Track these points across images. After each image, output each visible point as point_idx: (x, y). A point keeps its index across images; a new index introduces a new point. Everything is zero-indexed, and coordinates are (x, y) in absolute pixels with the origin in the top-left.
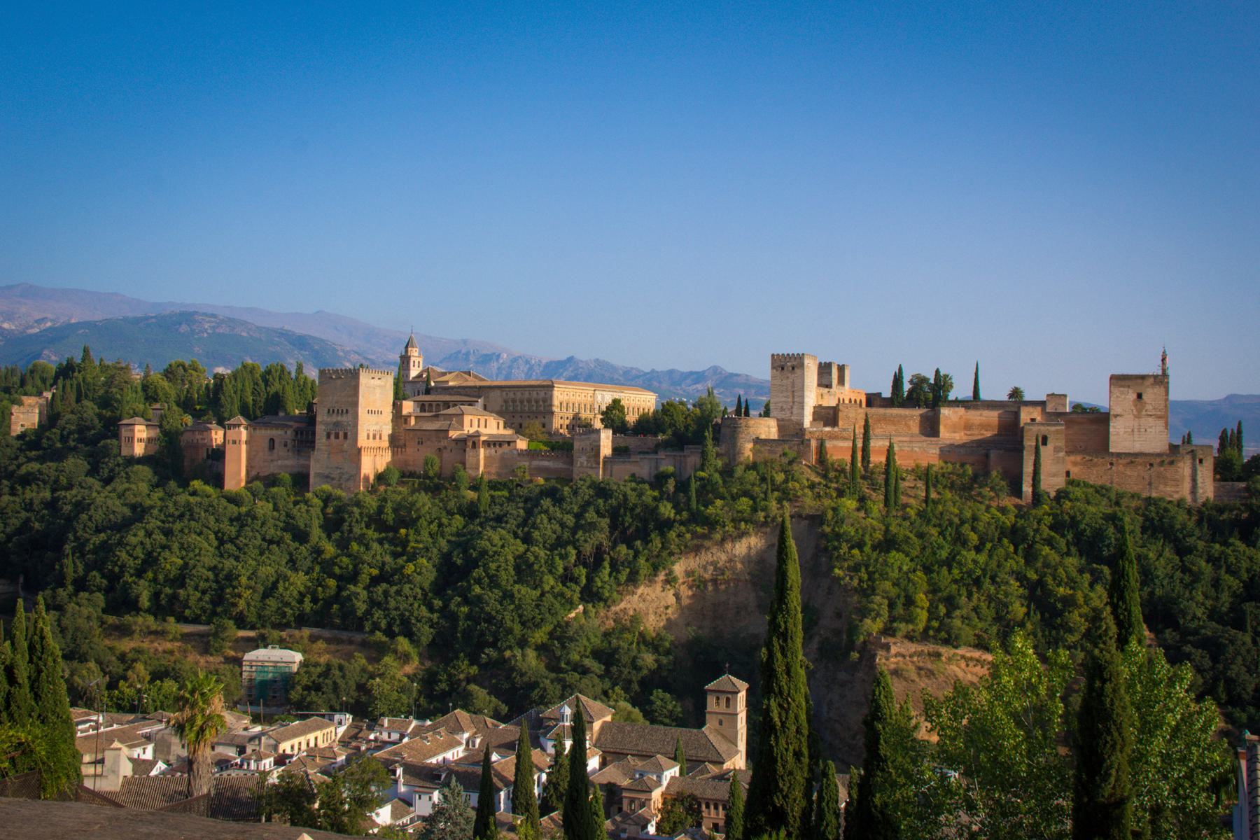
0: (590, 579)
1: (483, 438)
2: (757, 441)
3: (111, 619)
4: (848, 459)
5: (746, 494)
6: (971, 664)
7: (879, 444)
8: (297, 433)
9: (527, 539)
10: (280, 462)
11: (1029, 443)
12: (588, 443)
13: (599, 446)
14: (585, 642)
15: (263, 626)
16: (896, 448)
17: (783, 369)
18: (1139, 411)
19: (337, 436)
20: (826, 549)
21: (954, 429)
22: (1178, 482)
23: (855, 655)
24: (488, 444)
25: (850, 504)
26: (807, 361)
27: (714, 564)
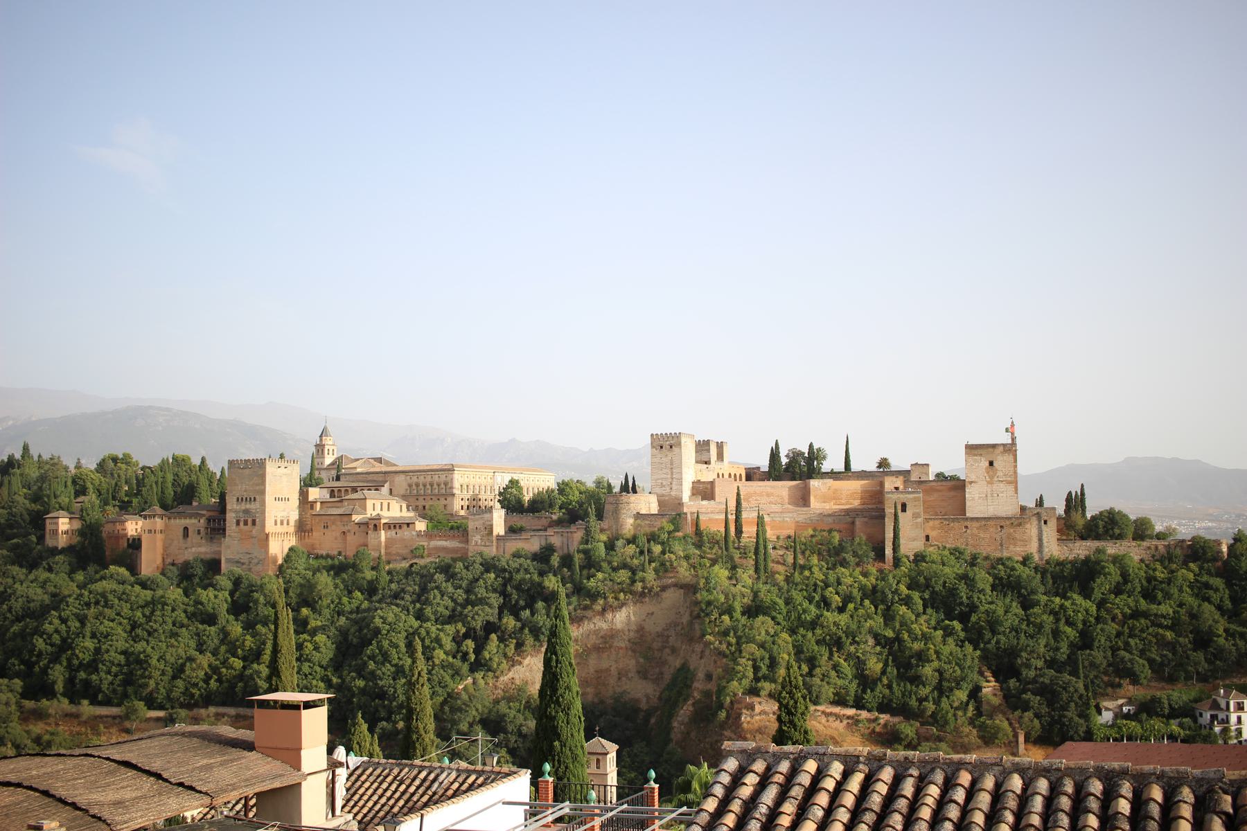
0: (478, 650)
1: (383, 521)
2: (638, 516)
3: (29, 704)
4: (723, 530)
5: (625, 566)
6: (831, 719)
7: (748, 515)
8: (209, 520)
9: (420, 616)
10: (194, 549)
11: (889, 510)
12: (481, 522)
13: (492, 525)
14: (474, 713)
15: (173, 708)
16: (767, 519)
17: (661, 447)
18: (992, 477)
19: (246, 523)
20: (698, 616)
21: (825, 499)
22: (1026, 542)
23: (723, 715)
24: (389, 526)
25: (721, 573)
26: (683, 440)
27: (596, 632)
